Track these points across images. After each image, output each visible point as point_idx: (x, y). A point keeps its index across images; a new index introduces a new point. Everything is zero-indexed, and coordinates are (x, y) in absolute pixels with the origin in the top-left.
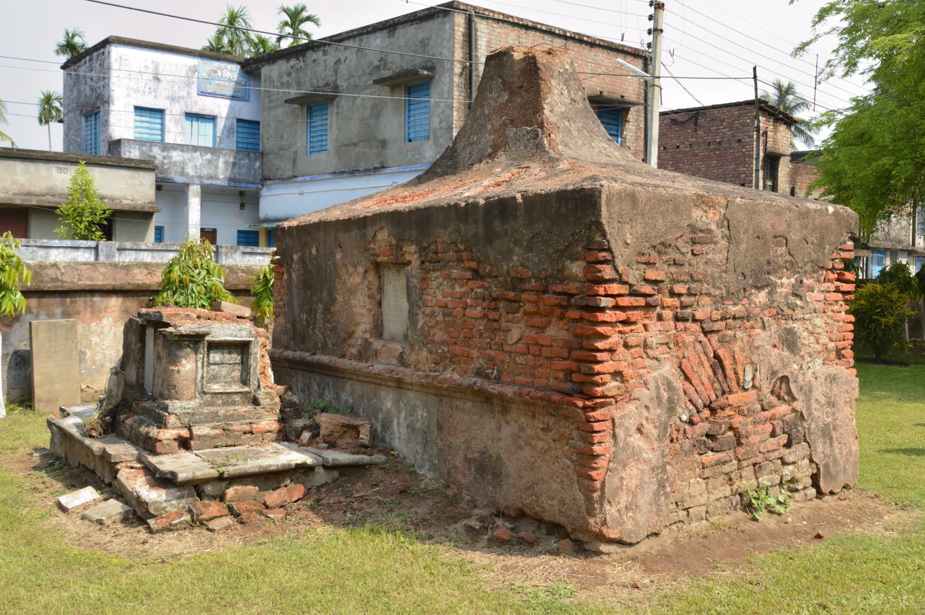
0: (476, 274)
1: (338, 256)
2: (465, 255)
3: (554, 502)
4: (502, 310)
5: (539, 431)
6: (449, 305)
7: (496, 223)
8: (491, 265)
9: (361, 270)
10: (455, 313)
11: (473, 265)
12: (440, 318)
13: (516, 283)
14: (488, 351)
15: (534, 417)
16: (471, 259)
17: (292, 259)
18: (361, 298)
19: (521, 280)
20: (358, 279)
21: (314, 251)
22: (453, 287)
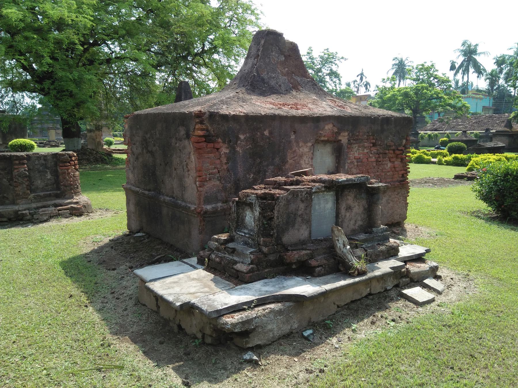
0: (374, 145)
1: (293, 137)
2: (371, 137)
3: (398, 216)
4: (381, 157)
5: (396, 195)
6: (361, 158)
7: (385, 126)
8: (381, 141)
9: (310, 144)
10: (363, 161)
11: (374, 141)
12: (356, 164)
13: (388, 147)
14: (377, 173)
15: (394, 191)
16: (373, 139)
17: (238, 138)
18: (307, 160)
19: (390, 146)
20: (306, 150)
21: (266, 133)
22: (363, 150)
